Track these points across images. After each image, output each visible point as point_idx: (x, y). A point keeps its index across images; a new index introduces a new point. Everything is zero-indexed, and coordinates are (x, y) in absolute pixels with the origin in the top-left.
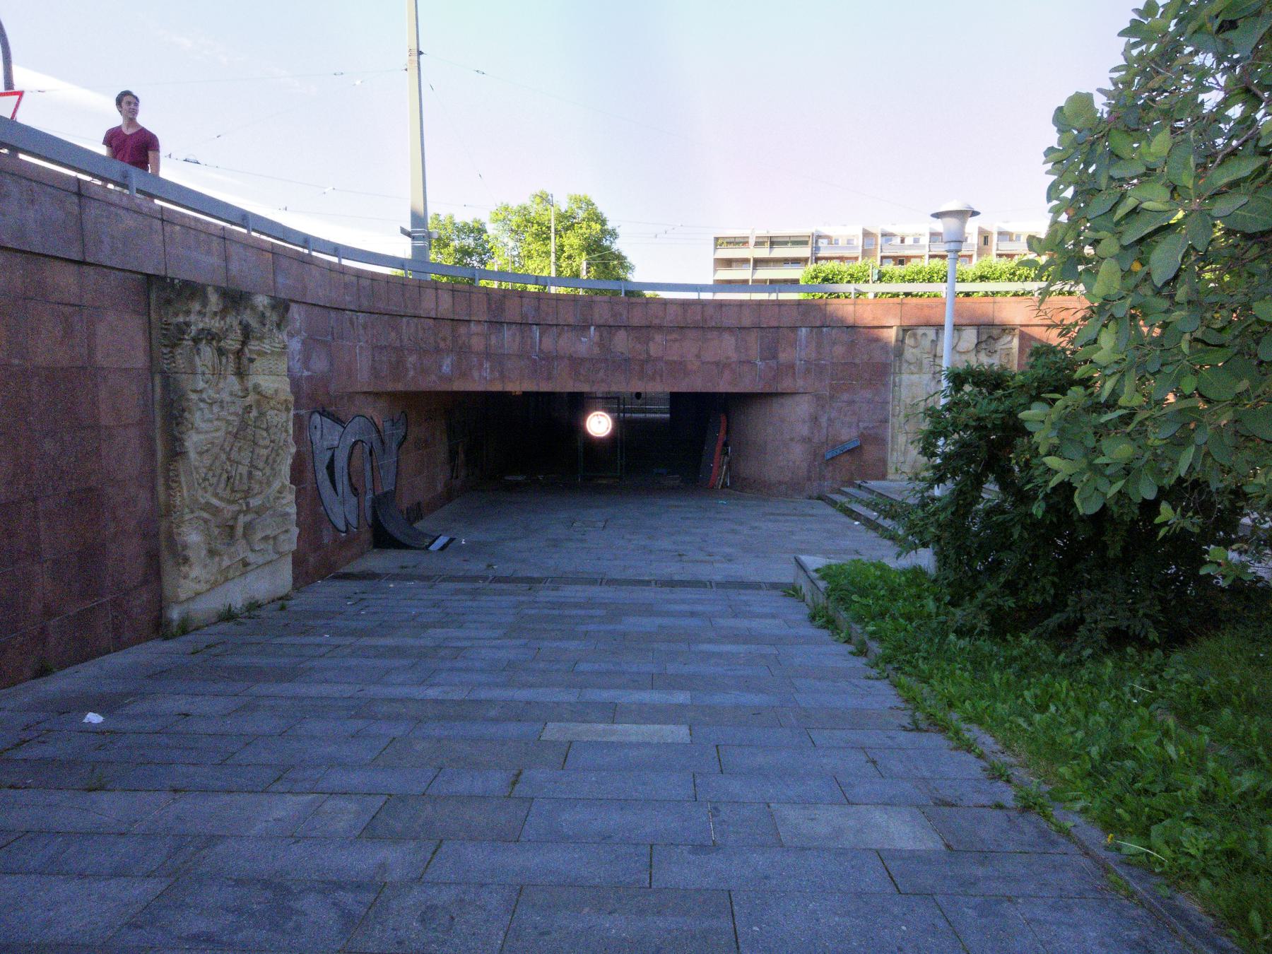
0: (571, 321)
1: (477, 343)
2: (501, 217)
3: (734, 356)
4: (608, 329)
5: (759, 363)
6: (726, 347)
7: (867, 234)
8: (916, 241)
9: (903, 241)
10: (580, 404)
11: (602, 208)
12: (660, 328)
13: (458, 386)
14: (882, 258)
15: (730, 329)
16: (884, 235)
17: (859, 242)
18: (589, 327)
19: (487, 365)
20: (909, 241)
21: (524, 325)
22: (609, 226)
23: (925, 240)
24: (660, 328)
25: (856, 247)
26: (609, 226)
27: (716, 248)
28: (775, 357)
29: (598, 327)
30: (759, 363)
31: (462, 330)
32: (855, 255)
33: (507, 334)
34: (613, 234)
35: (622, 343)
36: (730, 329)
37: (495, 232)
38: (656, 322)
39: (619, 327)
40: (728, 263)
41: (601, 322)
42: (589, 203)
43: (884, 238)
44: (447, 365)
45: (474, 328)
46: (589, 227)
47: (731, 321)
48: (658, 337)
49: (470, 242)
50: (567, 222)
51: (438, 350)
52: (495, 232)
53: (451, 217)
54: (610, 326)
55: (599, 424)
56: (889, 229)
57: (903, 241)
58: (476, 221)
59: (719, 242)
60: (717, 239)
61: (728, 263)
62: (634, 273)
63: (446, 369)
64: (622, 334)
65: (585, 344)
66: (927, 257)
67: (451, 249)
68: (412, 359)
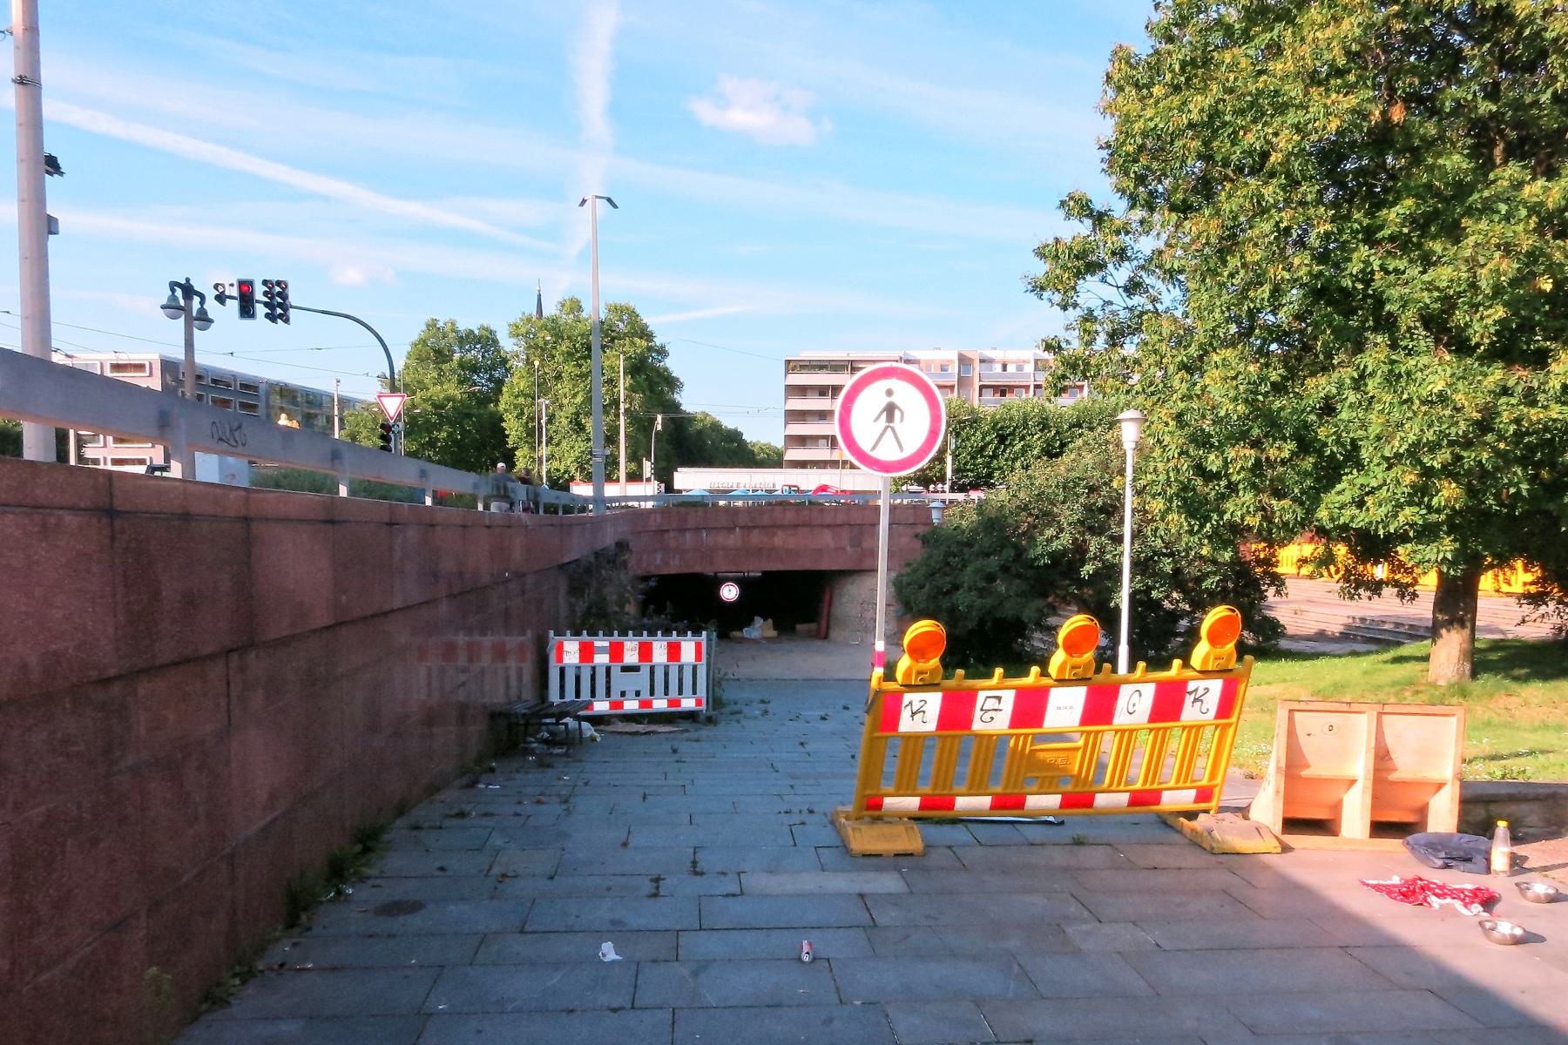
0: (725, 524)
1: (672, 544)
2: (523, 330)
3: (832, 545)
4: (747, 528)
5: (848, 548)
6: (827, 539)
7: (964, 361)
8: (1020, 368)
9: (1004, 367)
10: (718, 582)
11: (650, 320)
12: (782, 527)
13: (665, 572)
14: (982, 387)
15: (828, 526)
16: (982, 361)
17: (954, 369)
18: (734, 528)
19: (677, 557)
20: (1011, 368)
21: (698, 529)
22: (658, 341)
23: (1029, 368)
24: (782, 527)
25: (951, 375)
26: (658, 341)
27: (787, 372)
28: (859, 545)
29: (742, 528)
30: (848, 548)
31: (666, 536)
32: (951, 383)
33: (688, 535)
34: (662, 352)
35: (756, 538)
36: (828, 526)
37: (516, 348)
38: (779, 523)
39: (754, 527)
40: (802, 391)
41: (742, 524)
42: (633, 314)
43: (983, 364)
44: (659, 558)
45: (672, 534)
46: (633, 344)
47: (828, 519)
48: (780, 533)
49: (475, 354)
50: (609, 335)
51: (656, 551)
52: (516, 348)
53: (453, 324)
54: (749, 527)
55: (730, 592)
56: (989, 354)
57: (1004, 367)
58: (482, 328)
59: (792, 366)
60: (788, 362)
61: (802, 391)
62: (682, 393)
63: (658, 561)
64: (756, 532)
65: (733, 540)
66: (1032, 388)
67: (455, 364)
68: (645, 557)
